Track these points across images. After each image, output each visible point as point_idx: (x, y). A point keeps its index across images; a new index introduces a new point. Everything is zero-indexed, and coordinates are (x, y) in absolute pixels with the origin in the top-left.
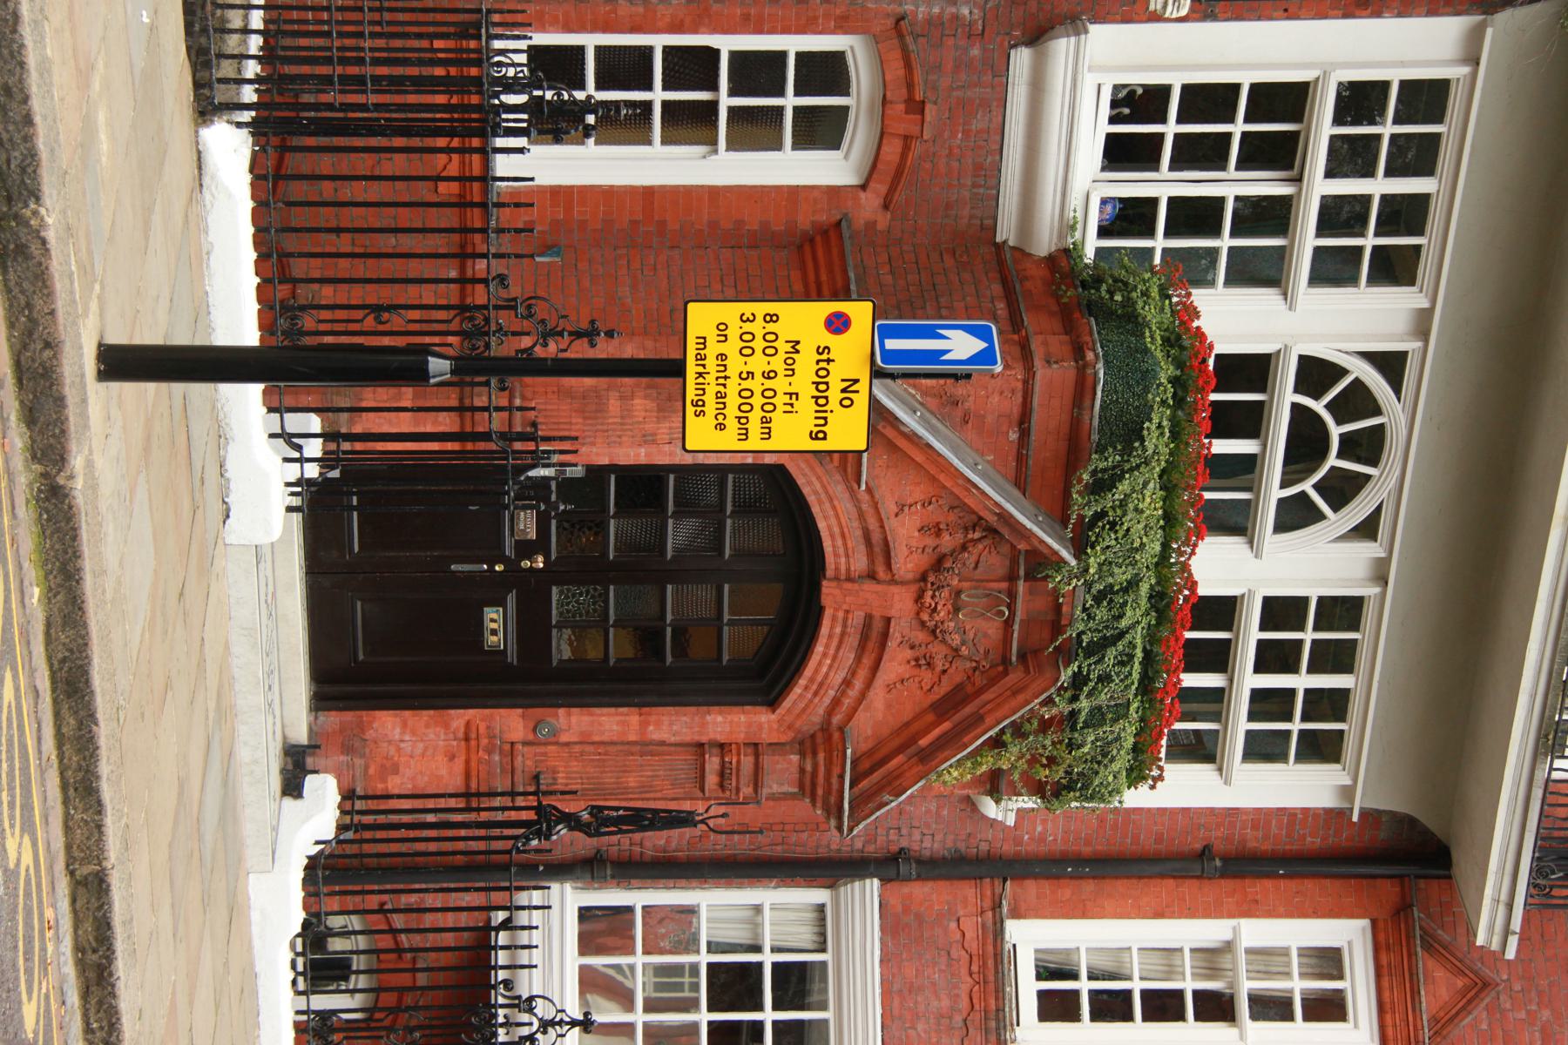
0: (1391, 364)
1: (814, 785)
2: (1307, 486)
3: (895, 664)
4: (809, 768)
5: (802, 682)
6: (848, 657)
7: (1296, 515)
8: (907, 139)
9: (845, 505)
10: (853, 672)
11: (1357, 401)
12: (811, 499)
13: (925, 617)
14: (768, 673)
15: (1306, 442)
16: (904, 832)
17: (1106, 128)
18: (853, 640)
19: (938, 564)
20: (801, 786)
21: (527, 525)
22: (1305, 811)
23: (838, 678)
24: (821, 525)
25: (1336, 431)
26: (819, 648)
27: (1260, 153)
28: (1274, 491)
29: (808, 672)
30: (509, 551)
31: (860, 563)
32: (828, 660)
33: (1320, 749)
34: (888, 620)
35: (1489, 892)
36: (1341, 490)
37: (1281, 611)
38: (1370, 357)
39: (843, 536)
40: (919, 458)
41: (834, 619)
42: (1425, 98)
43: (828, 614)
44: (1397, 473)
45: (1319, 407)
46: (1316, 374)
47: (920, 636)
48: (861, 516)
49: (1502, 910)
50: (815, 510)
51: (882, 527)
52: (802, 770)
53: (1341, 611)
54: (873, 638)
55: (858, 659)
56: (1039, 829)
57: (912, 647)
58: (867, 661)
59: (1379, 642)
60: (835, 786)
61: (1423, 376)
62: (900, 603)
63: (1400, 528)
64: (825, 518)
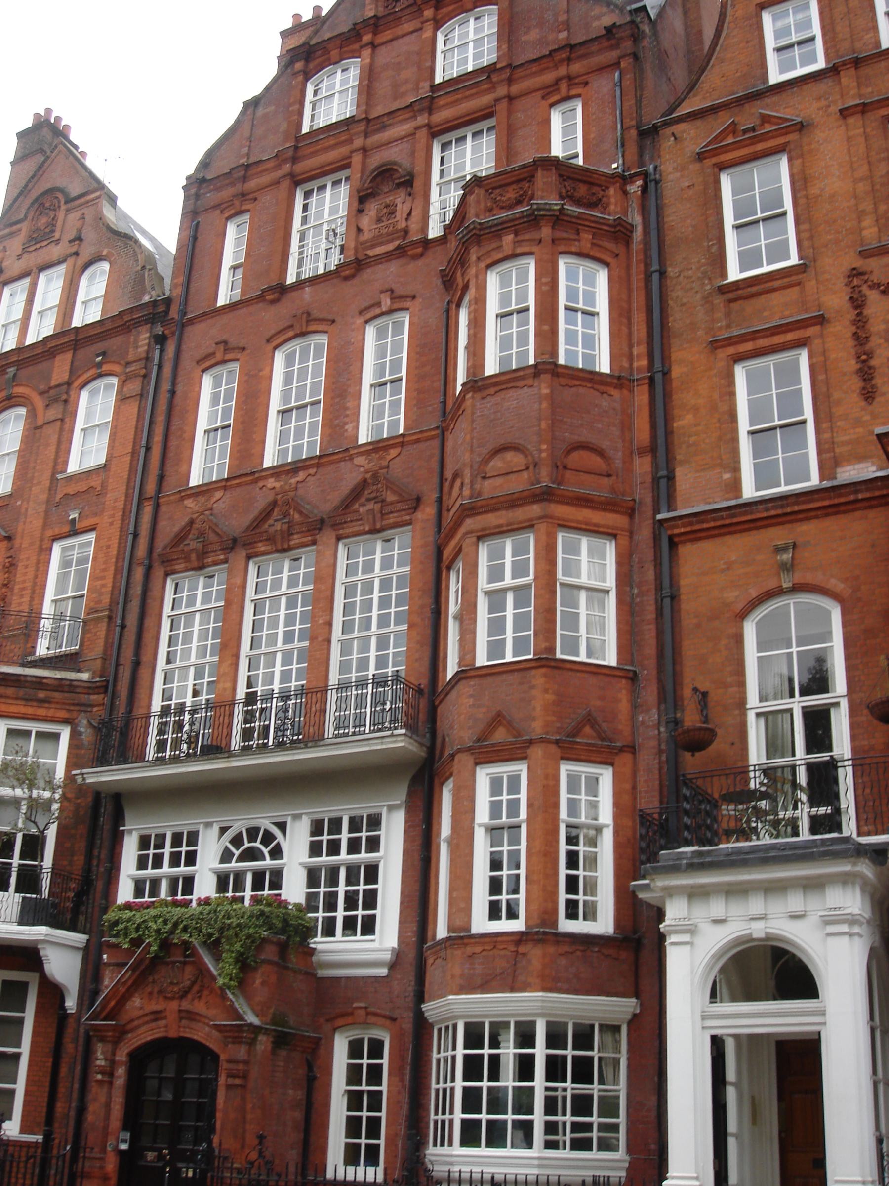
0: (223, 830)
1: (236, 1037)
2: (266, 851)
3: (200, 1007)
4: (230, 1040)
5: (208, 1044)
6: (200, 1024)
7: (277, 853)
8: (368, 1014)
9: (143, 1029)
10: (204, 1023)
11: (237, 841)
12: (139, 1043)
13: (177, 996)
14: (206, 1057)
15: (251, 855)
16: (407, 994)
17: (359, 937)
18: (194, 1025)
19: (160, 992)
20: (240, 1043)
21: (151, 1156)
22: (406, 822)
23: (207, 1029)
24: (149, 1038)
25: (247, 845)
26: (195, 1037)
27: (333, 880)
28: (268, 862)
29: (204, 1042)
30: (160, 1164)
31: (162, 1023)
32: (200, 1033)
33: (375, 822)
34: (180, 1011)
35: (379, 747)
36: (268, 838)
37: (315, 849)
38: (220, 838)
39: (152, 1030)
40: (112, 1003)
41: (184, 1032)
42: (144, 843)
43: (182, 1034)
44: (261, 820)
45: (237, 853)
46: (226, 857)
47: (190, 996)
48: (147, 1023)
49: (384, 740)
50: (143, 1041)
51: (146, 1015)
52: (233, 1043)
53: (317, 828)
54: (190, 1016)
55: (199, 1021)
56: (409, 934)
57: (193, 1000)
58: (198, 1018)
59: (326, 811)
60: (228, 1028)
61: (225, 819)
62: (174, 1005)
63: (279, 814)
64: (145, 1037)
